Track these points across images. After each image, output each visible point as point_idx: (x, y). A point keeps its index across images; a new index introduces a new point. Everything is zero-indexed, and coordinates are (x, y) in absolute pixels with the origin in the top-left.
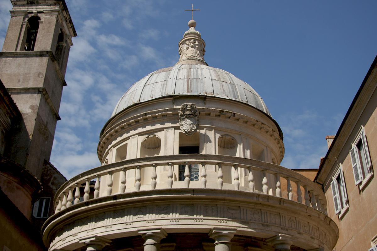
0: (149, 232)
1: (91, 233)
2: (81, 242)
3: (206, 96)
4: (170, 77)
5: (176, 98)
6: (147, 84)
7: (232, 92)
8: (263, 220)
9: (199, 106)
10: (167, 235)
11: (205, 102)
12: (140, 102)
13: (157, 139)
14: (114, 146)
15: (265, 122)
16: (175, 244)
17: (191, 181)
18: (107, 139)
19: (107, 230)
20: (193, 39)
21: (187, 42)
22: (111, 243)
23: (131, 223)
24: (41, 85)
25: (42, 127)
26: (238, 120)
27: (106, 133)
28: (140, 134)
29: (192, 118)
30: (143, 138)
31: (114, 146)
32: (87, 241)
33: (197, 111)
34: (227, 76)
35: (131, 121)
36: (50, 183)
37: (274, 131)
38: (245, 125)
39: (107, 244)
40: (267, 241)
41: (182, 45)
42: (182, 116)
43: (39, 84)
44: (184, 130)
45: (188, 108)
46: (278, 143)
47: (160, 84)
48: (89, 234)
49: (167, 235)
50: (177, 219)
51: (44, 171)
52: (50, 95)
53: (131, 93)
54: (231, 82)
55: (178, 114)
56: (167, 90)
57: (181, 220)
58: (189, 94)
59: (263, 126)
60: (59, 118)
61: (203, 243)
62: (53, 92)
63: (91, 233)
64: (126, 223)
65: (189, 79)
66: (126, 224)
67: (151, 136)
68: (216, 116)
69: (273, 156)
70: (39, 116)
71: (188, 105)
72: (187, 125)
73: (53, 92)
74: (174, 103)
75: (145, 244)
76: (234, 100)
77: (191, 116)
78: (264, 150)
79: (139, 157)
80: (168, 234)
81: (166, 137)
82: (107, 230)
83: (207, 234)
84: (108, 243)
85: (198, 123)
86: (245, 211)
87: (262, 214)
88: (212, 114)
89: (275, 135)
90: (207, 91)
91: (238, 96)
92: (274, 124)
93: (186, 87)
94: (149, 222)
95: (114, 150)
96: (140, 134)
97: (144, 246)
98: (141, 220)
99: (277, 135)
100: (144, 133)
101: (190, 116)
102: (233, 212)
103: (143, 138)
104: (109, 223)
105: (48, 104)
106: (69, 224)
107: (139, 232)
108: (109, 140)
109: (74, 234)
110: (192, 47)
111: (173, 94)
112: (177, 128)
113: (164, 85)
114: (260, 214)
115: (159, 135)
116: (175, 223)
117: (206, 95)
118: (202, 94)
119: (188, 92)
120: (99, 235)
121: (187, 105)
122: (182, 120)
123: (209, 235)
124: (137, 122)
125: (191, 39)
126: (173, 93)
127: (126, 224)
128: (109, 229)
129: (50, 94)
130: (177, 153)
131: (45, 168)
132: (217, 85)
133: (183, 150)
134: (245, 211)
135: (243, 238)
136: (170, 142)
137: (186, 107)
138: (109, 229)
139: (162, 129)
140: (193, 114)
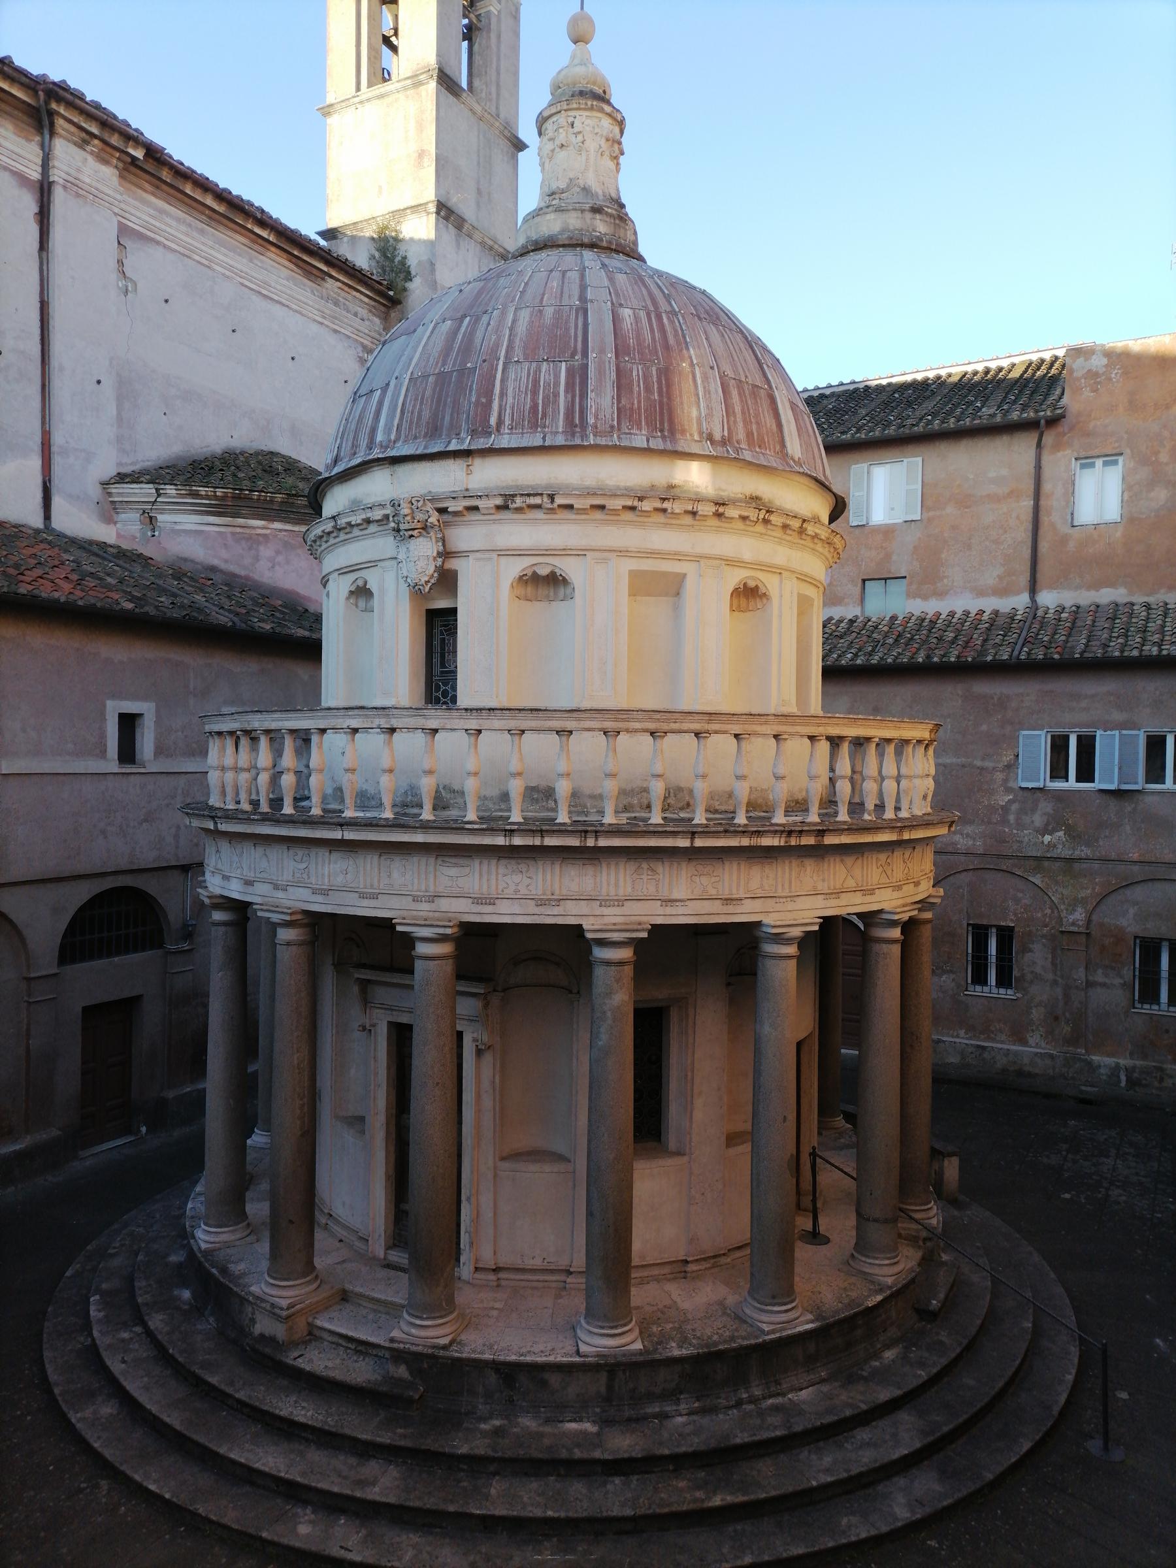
29: (421, 539)
68: (498, 508)
77: (415, 533)
88: (483, 511)
101: (410, 533)
102: (453, 871)
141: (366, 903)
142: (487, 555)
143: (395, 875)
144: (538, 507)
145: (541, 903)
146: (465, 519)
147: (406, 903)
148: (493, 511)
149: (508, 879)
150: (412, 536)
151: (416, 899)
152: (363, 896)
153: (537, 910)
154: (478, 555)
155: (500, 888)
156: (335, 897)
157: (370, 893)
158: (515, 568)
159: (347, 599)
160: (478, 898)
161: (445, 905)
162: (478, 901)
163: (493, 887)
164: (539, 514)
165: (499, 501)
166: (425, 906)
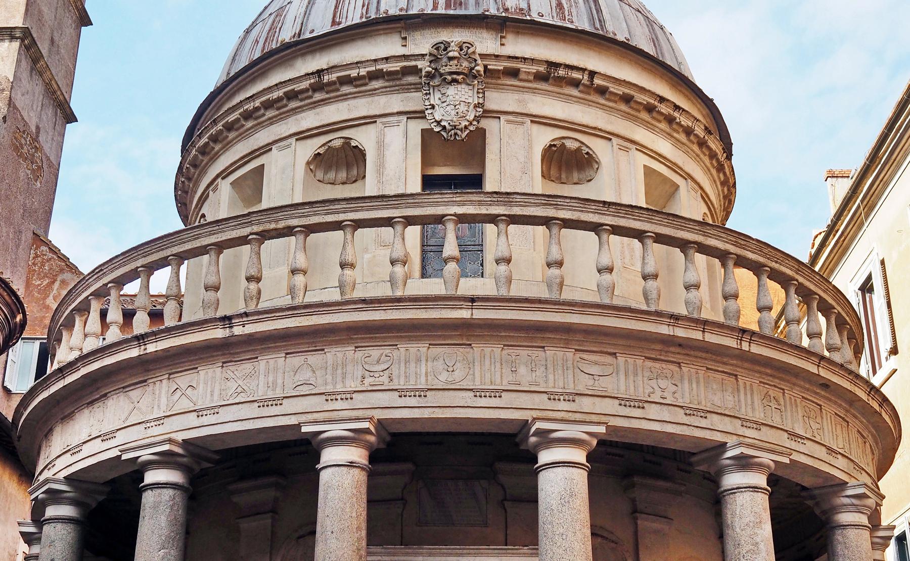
0: (335, 430)
2: (124, 457)
3: (506, 19)
10: (388, 438)
11: (502, 37)
13: (356, 151)
14: (224, 174)
16: (409, 466)
17: (462, 280)
18: (203, 151)
19: (205, 420)
22: (217, 462)
23: (279, 402)
24: (17, 21)
25: (23, 142)
27: (200, 136)
28: (302, 136)
29: (463, 86)
30: (313, 146)
31: (224, 174)
32: (145, 455)
33: (479, 62)
36: (51, 297)
39: (206, 465)
40: (694, 459)
42: (430, 76)
43: (14, 17)
44: (439, 123)
46: (720, 168)
48: (150, 432)
49: (388, 438)
50: (422, 390)
51: (34, 264)
52: (45, 52)
53: (273, 17)
57: (433, 392)
58: (452, 12)
59: (676, 114)
60: (71, 118)
61: (499, 466)
62: (52, 41)
64: (261, 401)
66: (261, 404)
70: (15, 107)
71: (452, 44)
73: (52, 41)
74: (405, 38)
75: (319, 466)
77: (460, 77)
79: (298, 199)
80: (393, 435)
81: (381, 145)
82: (205, 420)
83: (515, 435)
84: (208, 460)
85: (481, 101)
88: (522, 76)
90: (509, 4)
94: (334, 397)
95: (225, 186)
96: (302, 136)
97: (317, 473)
98: (307, 393)
101: (455, 76)
105: (41, 74)
106: (88, 404)
108: (208, 154)
109: (105, 434)
111: (403, 13)
112: (419, 115)
115: (364, 138)
116: (413, 402)
117: (504, 14)
119: (448, 6)
120: (180, 437)
121: (447, 46)
122: (431, 91)
123: (517, 440)
126: (401, 10)
127: (261, 404)
129: (44, 47)
130: (415, 186)
131: (37, 256)
133: (430, 183)
135: (615, 451)
136: (395, 161)
137: (445, 49)
139: (370, 120)
142: (519, 119)
143: (522, 370)
144: (576, 84)
145: (690, 411)
146: (499, 82)
147: (540, 401)
148: (531, 78)
149: (653, 383)
150: (455, 81)
152: (478, 392)
153: (686, 420)
154: (510, 118)
155: (647, 391)
156: (433, 398)
157: (492, 390)
158: (545, 137)
159: (308, 163)
160: (628, 400)
162: (624, 402)
163: (641, 390)
164: (575, 92)
165: (542, 69)
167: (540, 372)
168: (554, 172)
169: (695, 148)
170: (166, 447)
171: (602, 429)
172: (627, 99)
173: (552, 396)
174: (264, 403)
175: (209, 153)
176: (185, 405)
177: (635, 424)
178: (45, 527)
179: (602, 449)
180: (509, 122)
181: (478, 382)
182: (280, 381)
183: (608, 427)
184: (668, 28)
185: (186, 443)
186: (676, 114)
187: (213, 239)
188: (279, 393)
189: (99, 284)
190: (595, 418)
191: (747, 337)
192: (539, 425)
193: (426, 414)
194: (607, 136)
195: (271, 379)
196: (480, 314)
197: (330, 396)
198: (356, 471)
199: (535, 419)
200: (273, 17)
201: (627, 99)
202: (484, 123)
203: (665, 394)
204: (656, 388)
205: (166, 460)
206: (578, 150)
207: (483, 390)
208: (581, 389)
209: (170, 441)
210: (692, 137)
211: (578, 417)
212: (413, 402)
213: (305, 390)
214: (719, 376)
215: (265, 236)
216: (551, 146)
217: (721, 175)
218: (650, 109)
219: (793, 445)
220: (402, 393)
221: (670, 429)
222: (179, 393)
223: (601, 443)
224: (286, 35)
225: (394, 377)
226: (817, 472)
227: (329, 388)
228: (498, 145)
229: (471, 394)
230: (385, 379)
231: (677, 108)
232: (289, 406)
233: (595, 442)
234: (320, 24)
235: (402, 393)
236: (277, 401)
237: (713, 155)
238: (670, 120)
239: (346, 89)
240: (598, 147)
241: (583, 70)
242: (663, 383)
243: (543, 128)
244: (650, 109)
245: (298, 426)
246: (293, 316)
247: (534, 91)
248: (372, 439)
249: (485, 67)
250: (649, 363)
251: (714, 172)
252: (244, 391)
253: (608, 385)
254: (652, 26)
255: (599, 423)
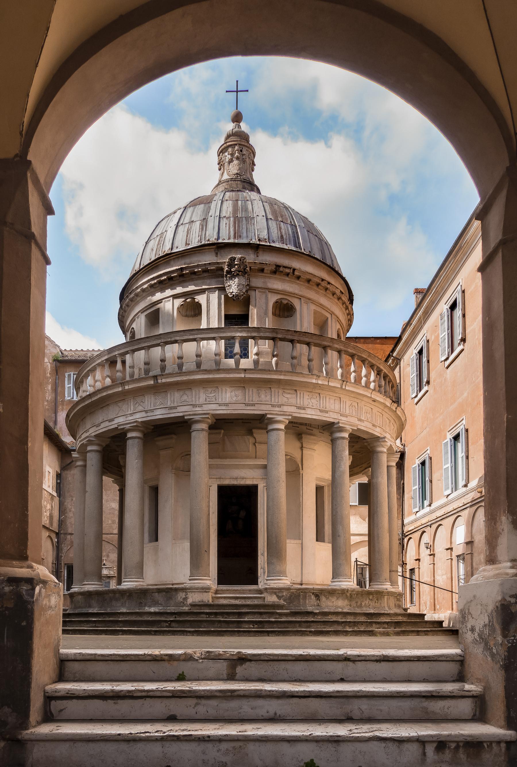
0: (197, 418)
1: (130, 418)
4: (210, 214)
5: (219, 247)
6: (180, 224)
7: (292, 239)
8: (321, 405)
9: (250, 257)
10: (215, 421)
12: (173, 251)
15: (332, 281)
20: (239, 144)
21: (230, 150)
26: (298, 278)
28: (175, 297)
34: (286, 212)
35: (163, 278)
37: (342, 293)
38: (307, 284)
41: (223, 153)
45: (236, 263)
47: (198, 224)
49: (215, 421)
53: (159, 237)
54: (291, 222)
55: (222, 269)
56: (207, 235)
59: (328, 286)
63: (130, 418)
65: (236, 218)
67: (188, 300)
69: (338, 326)
72: (233, 287)
76: (294, 249)
78: (328, 318)
80: (216, 419)
82: (149, 414)
86: (302, 395)
87: (320, 398)
89: (343, 299)
91: (299, 243)
92: (342, 282)
93: (232, 230)
96: (175, 297)
97: (190, 434)
99: (345, 298)
100: (180, 295)
102: (288, 396)
103: (178, 302)
104: (151, 407)
107: (185, 418)
108: (134, 301)
110: (238, 158)
113: (202, 226)
114: (318, 398)
115: (201, 299)
117: (258, 243)
118: (255, 241)
120: (140, 420)
124: (170, 279)
125: (236, 144)
128: (152, 414)
132: (273, 225)
134: (302, 395)
138: (152, 414)
139: (203, 291)
140: (243, 270)
141: (249, 408)
143: (263, 396)
147: (269, 408)
149: (309, 401)
151: (273, 406)
154: (260, 290)
156: (231, 407)
161: (285, 409)
166: (277, 409)
167: (268, 397)
168: (277, 312)
169: (336, 300)
170: (135, 424)
171: (290, 417)
172: (309, 281)
173: (273, 406)
174: (171, 408)
175: (134, 301)
176: (140, 408)
177: (302, 416)
178: (88, 454)
179: (291, 425)
180: (259, 292)
181: (247, 400)
182: (176, 400)
183: (292, 417)
184: (330, 242)
185: (142, 422)
186: (328, 286)
187: (146, 344)
188: (176, 405)
189: (100, 361)
190: (288, 413)
191: (345, 383)
192: (268, 416)
193: (229, 412)
194: (300, 297)
195: (172, 399)
196: (247, 376)
197: (194, 406)
198: (204, 432)
199: (266, 414)
200: (159, 237)
201: (309, 281)
202: (250, 293)
203: (313, 405)
204: (310, 402)
205: (134, 429)
206: (287, 303)
207: (249, 404)
208: (283, 403)
209: (136, 422)
210: (335, 296)
211: (282, 413)
212: (224, 408)
213: (185, 403)
214: (334, 398)
215: (167, 343)
216: (276, 302)
217: (347, 311)
218: (318, 285)
219: (359, 423)
220: (220, 405)
221: (314, 417)
222: (138, 404)
223: (289, 422)
224: (167, 248)
225: (217, 399)
226: (368, 433)
227: (194, 403)
228: (254, 302)
229: (244, 405)
230: (214, 399)
231: (329, 283)
232: (180, 409)
233: (287, 422)
234: (180, 247)
235: (220, 405)
236: (175, 408)
237: (344, 303)
238: (326, 289)
239: (194, 276)
240: (296, 303)
241: (290, 268)
242: (313, 401)
243: (273, 294)
244: (318, 285)
245: (183, 416)
246: (180, 376)
247: (269, 278)
248: (209, 421)
249: (250, 268)
250: (308, 393)
251: (344, 310)
252: (162, 404)
253: (293, 401)
254: (321, 243)
255: (289, 415)
